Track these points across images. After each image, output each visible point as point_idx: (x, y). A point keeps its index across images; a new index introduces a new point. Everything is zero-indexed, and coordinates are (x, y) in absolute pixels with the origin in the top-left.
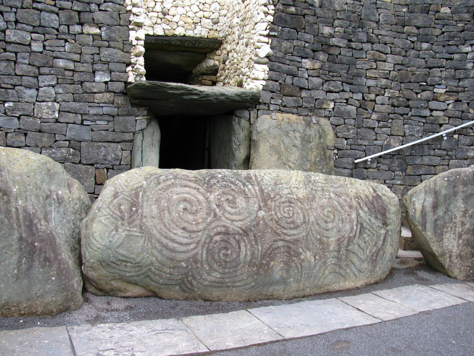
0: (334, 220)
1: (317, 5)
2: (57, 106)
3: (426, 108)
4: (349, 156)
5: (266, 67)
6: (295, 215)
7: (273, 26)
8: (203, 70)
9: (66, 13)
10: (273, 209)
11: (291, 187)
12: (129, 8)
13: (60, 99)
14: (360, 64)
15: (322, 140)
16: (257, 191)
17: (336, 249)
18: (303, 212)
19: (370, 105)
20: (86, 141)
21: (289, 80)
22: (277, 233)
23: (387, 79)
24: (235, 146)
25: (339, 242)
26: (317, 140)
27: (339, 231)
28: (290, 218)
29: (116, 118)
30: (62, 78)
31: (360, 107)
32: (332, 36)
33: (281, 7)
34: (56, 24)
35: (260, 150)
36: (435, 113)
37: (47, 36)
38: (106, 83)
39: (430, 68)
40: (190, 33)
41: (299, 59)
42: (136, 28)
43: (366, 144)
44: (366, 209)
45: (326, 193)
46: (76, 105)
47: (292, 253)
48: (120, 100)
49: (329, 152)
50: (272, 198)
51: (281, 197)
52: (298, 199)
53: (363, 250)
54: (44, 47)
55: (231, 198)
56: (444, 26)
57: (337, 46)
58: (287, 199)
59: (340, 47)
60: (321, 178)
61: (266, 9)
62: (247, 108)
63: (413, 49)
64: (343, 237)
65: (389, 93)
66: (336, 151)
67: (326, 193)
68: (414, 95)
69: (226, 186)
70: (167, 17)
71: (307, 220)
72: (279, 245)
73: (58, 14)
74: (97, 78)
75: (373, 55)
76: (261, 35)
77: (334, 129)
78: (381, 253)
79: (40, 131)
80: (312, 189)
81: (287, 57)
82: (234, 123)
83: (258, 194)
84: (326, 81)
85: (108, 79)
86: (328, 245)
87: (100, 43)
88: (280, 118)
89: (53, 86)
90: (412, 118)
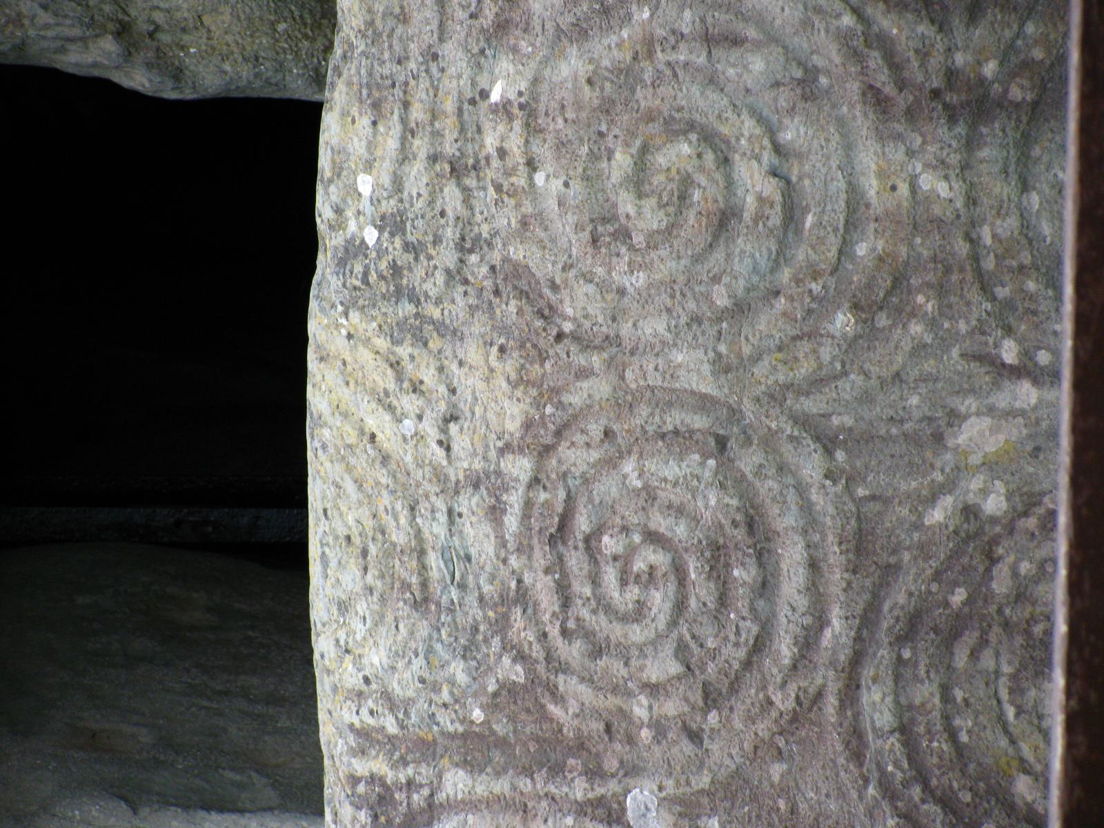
0: (708, 137)
6: (660, 522)
10: (612, 701)
11: (439, 476)
16: (480, 790)
17: (945, 137)
18: (641, 442)
22: (795, 718)
24: (139, 80)
25: (899, 102)
27: (807, 86)
28: (679, 571)
45: (490, 142)
47: (959, 597)
50: (533, 679)
51: (522, 597)
52: (541, 441)
58: (541, 556)
60: (358, 148)
64: (856, 56)
67: (490, 142)
71: (699, 422)
72: (885, 719)
80: (456, 276)
83: (501, 786)
86: (919, 218)
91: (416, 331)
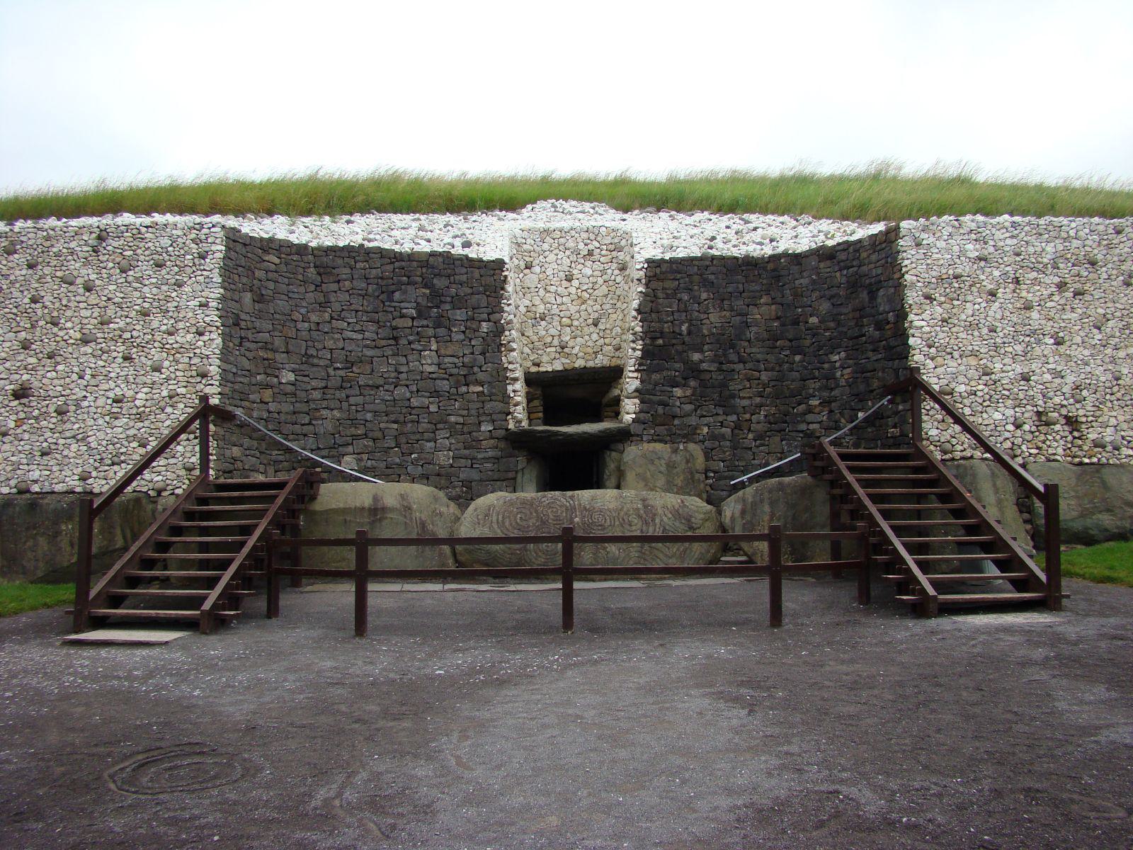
1: (685, 332)
2: (451, 453)
3: (803, 422)
4: (726, 478)
5: (637, 401)
7: (642, 361)
8: (605, 400)
9: (454, 378)
12: (505, 366)
13: (453, 449)
14: (733, 386)
15: (689, 465)
19: (745, 425)
20: (475, 481)
21: (660, 410)
23: (763, 397)
24: (605, 476)
26: (683, 466)
29: (500, 460)
30: (453, 430)
31: (736, 428)
32: (702, 361)
33: (648, 341)
34: (447, 388)
35: (627, 479)
36: (812, 427)
37: (441, 399)
38: (490, 431)
39: (805, 381)
40: (591, 364)
41: (669, 389)
42: (512, 382)
43: (744, 464)
44: (670, 516)
46: (467, 452)
48: (502, 445)
49: (697, 476)
53: (669, 549)
54: (439, 407)
55: (554, 510)
56: (814, 336)
57: (707, 371)
59: (711, 371)
61: (633, 345)
62: (621, 441)
63: (787, 362)
65: (765, 410)
66: (712, 475)
68: (791, 409)
69: (553, 503)
70: (566, 350)
73: (448, 380)
74: (483, 428)
75: (746, 374)
76: (630, 371)
77: (705, 453)
78: (688, 551)
79: (438, 475)
81: (657, 388)
82: (606, 456)
84: (699, 406)
85: (491, 428)
87: (483, 398)
88: (646, 448)
89: (448, 438)
90: (790, 434)
91: (616, 498)
